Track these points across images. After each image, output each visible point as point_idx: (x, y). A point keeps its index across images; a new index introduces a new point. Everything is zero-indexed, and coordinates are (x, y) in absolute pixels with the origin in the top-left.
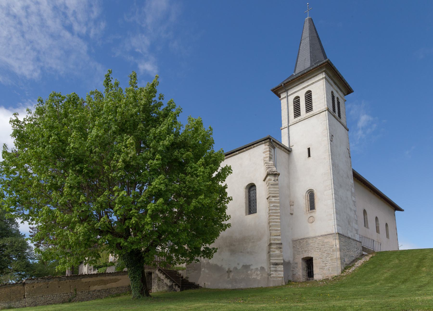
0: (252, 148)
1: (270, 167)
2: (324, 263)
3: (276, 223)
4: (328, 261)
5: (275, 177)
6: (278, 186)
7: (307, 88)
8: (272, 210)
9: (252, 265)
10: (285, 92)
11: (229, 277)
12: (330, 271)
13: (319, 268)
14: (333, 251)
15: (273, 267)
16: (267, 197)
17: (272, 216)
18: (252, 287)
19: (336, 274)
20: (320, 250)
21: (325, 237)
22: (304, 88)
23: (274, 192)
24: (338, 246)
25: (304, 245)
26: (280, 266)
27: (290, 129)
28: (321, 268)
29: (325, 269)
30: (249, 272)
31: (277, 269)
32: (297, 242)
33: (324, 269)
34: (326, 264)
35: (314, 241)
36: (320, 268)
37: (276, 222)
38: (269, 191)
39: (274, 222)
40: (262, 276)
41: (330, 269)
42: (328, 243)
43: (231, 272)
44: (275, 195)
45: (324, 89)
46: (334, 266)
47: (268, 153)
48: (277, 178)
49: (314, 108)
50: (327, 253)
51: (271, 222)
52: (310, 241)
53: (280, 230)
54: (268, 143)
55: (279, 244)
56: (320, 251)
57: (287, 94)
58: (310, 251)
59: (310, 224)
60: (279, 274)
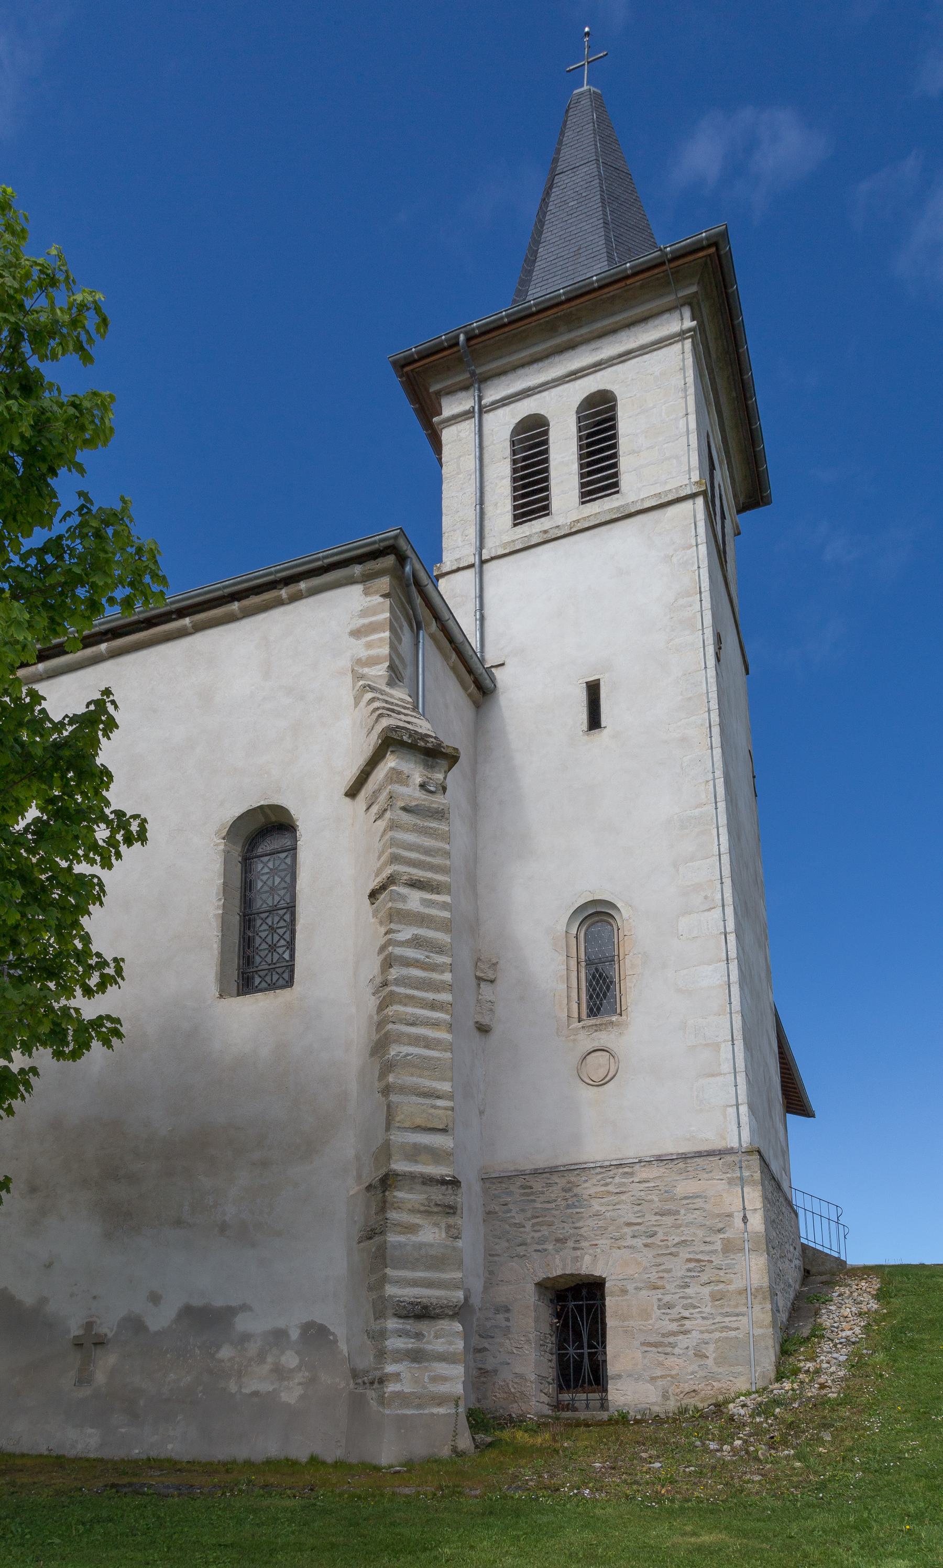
0: (280, 603)
1: (399, 713)
2: (674, 1313)
3: (427, 1047)
4: (695, 1307)
5: (430, 767)
6: (443, 827)
7: (591, 378)
8: (407, 963)
9: (245, 1308)
10: (466, 388)
11: (84, 1379)
12: (710, 1362)
13: (643, 1344)
14: (729, 1248)
15: (401, 1333)
16: (373, 884)
17: (400, 1003)
18: (241, 1452)
19: (743, 1379)
20: (649, 1241)
21: (682, 1165)
22: (574, 376)
23: (423, 857)
24: (757, 1222)
25: (553, 1205)
26: (444, 1325)
27: (487, 577)
28: (652, 1339)
29: (677, 1351)
30: (225, 1353)
31: (429, 1347)
32: (512, 1188)
33: (669, 1350)
34: (687, 1322)
35: (611, 1188)
36: (650, 1344)
37: (428, 1043)
38: (393, 842)
39: (416, 1041)
40: (313, 1380)
41: (710, 1350)
42: (699, 1203)
43: (100, 1343)
44: (429, 875)
45: (685, 390)
46: (733, 1334)
47: (381, 639)
48: (440, 776)
49: (626, 480)
50: (689, 1260)
51: (400, 1038)
52: (589, 1187)
53: (451, 1097)
54: (384, 583)
55: (443, 1182)
56: (646, 1245)
57: (480, 399)
58: (586, 1239)
59: (588, 1094)
60: (434, 1379)
